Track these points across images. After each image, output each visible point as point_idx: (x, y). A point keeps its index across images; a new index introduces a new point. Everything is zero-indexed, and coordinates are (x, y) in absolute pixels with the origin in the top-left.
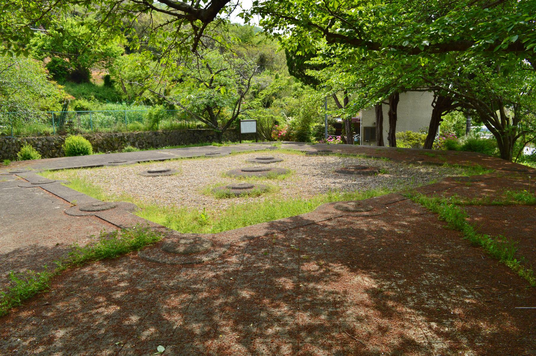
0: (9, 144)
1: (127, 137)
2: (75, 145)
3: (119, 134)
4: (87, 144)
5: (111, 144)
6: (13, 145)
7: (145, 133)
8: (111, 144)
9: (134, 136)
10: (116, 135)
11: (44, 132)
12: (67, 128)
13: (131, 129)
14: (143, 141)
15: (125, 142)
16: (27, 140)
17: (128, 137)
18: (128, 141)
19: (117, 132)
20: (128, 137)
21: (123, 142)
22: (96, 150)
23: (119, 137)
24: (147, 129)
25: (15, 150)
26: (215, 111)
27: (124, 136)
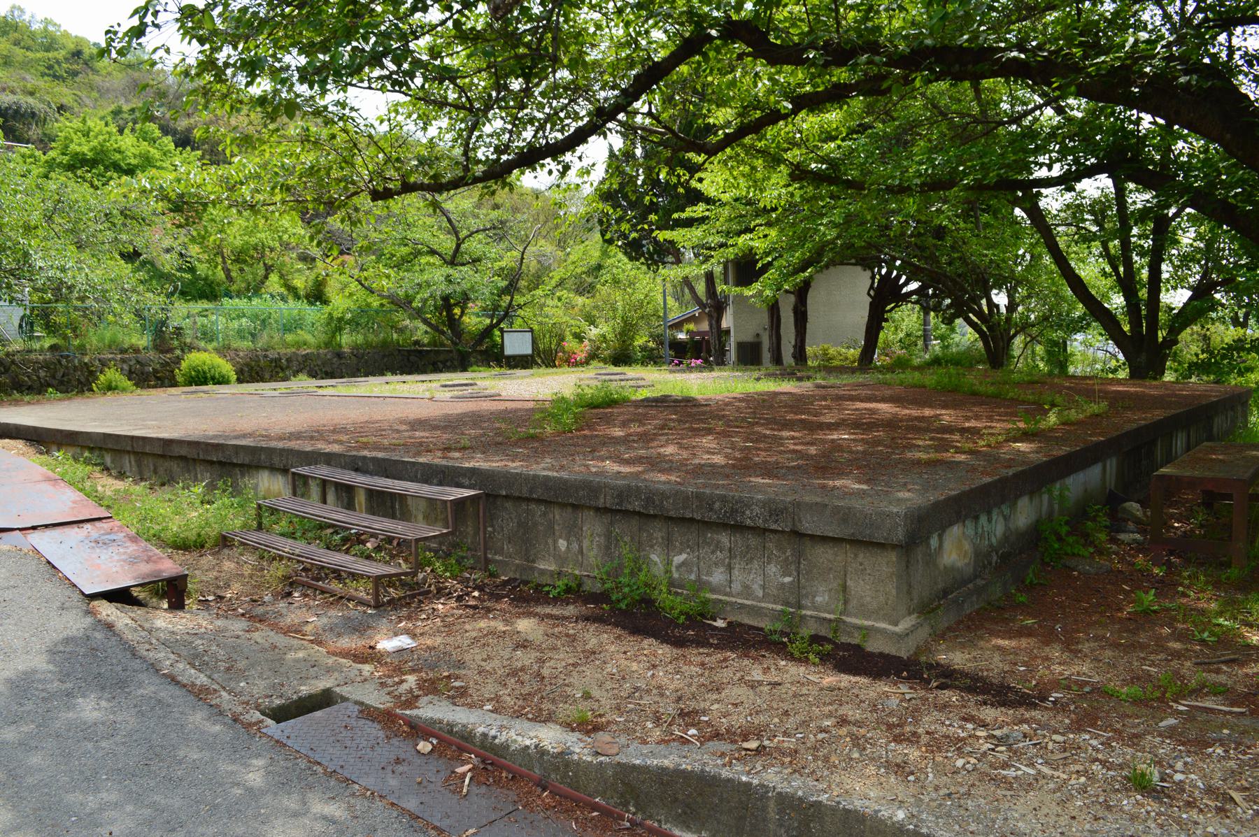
0: (67, 367)
1: (287, 360)
2: (206, 368)
3: (272, 354)
4: (227, 368)
5: (257, 373)
6: (75, 369)
7: (318, 354)
8: (257, 373)
9: (300, 359)
10: (266, 356)
11: (131, 346)
12: (172, 339)
13: (293, 346)
14: (317, 368)
15: (282, 369)
16: (99, 360)
17: (289, 360)
18: (288, 367)
19: (266, 351)
20: (289, 360)
21: (278, 370)
22: (240, 381)
23: (271, 361)
24: (322, 345)
25: (78, 380)
26: (670, 259)
27: (281, 359)
